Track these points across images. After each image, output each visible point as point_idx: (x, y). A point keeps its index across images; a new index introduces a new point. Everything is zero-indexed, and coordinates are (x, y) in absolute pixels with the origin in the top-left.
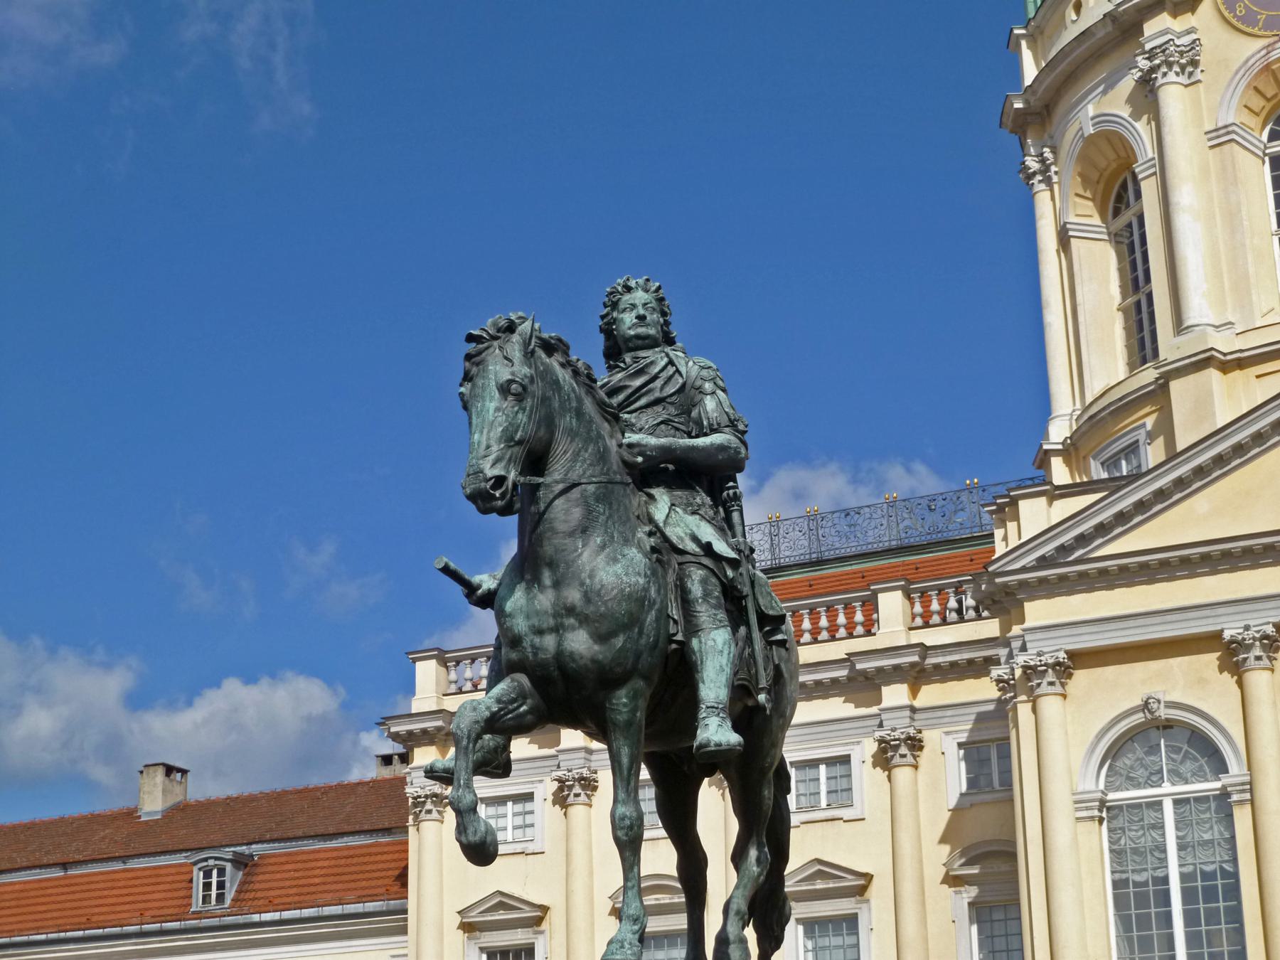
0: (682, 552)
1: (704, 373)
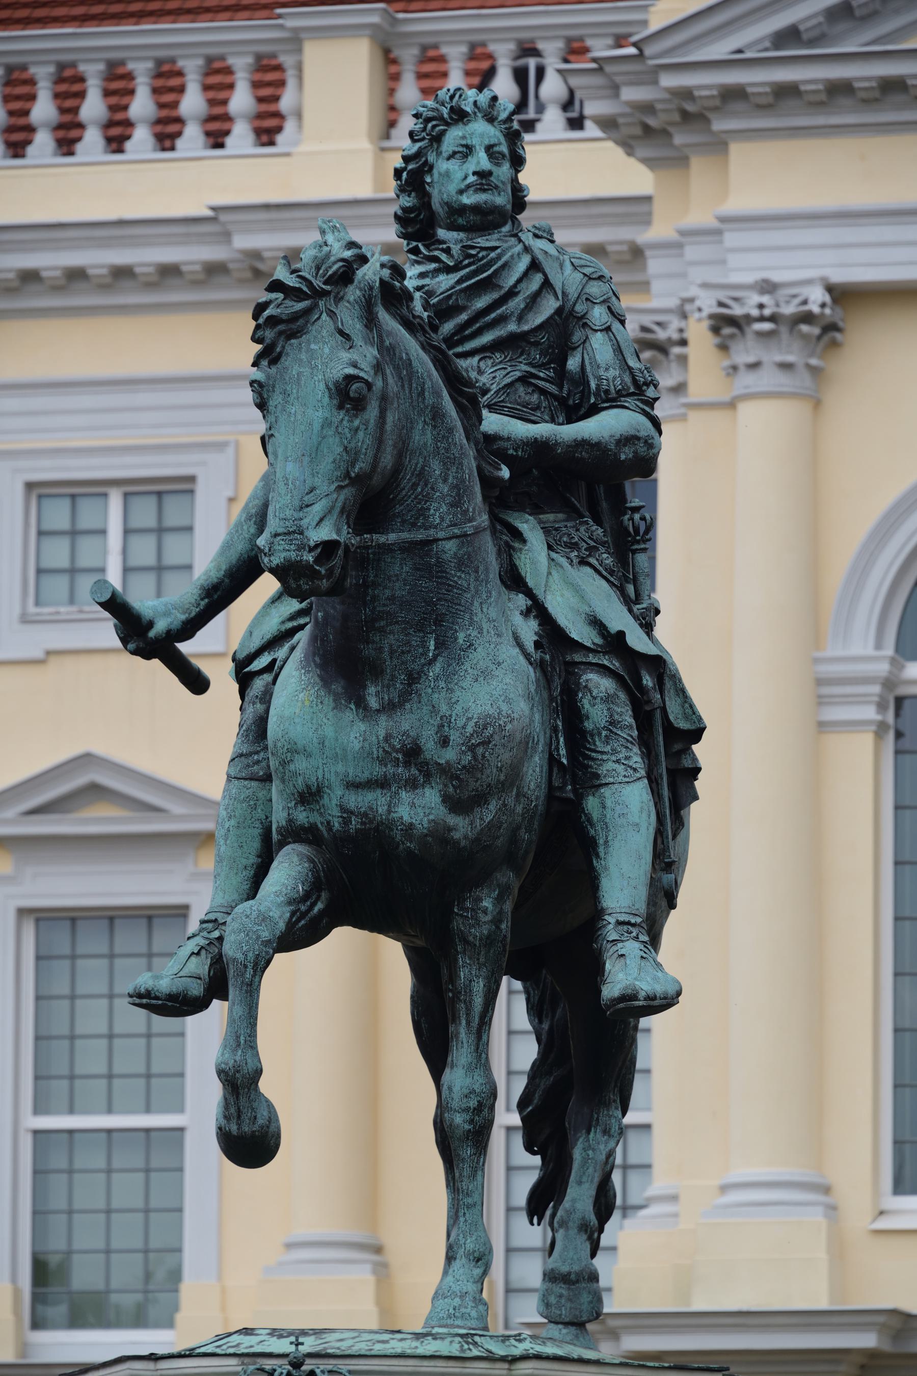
0: (577, 646)
1: (595, 289)
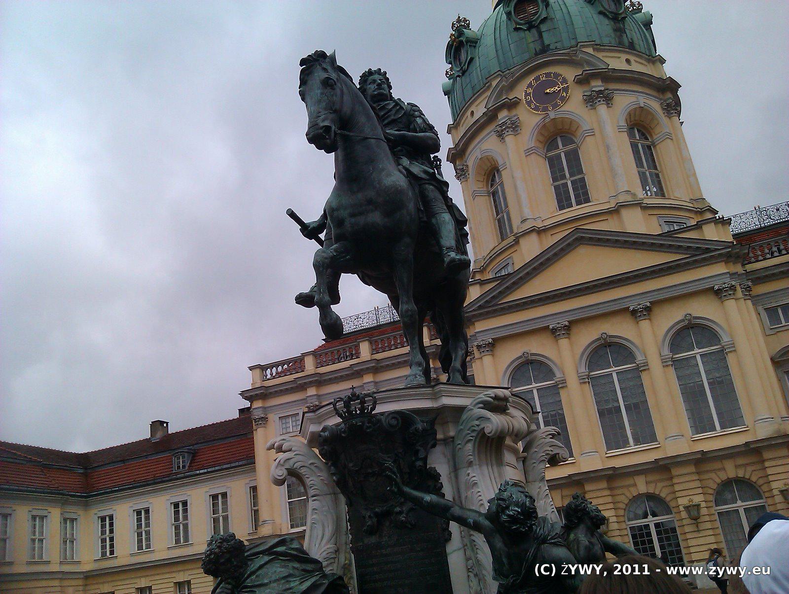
0: (421, 179)
1: (414, 108)
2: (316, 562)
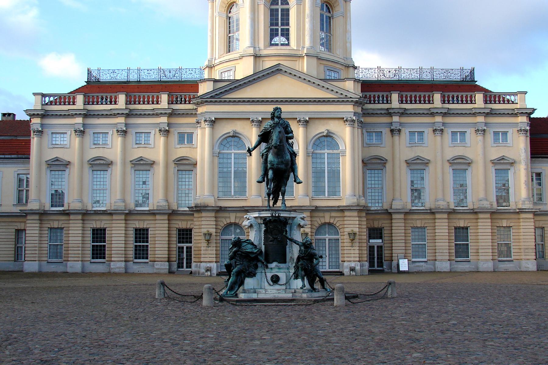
2: (255, 246)
